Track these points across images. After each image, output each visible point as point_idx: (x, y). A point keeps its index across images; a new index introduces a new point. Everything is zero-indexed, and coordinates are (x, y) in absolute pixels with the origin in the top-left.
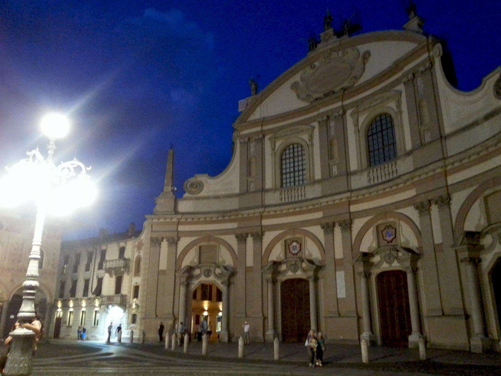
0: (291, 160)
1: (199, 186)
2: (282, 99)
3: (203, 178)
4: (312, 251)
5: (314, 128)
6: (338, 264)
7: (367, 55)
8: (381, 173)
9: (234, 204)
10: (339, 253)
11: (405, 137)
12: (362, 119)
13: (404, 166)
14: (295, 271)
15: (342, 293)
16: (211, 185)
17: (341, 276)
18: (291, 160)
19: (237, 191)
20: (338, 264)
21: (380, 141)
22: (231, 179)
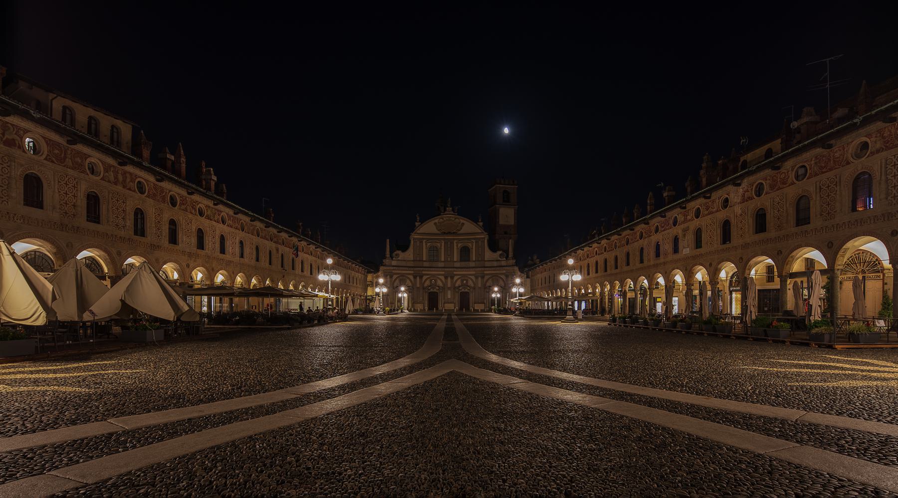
0: (434, 252)
1: (397, 255)
2: (430, 226)
3: (399, 252)
4: (440, 283)
6: (449, 288)
7: (463, 224)
8: (464, 264)
9: (411, 264)
10: (449, 286)
11: (473, 257)
13: (472, 264)
15: (449, 297)
16: (402, 255)
17: (449, 292)
18: (434, 252)
20: (449, 288)
21: (465, 253)
22: (409, 255)
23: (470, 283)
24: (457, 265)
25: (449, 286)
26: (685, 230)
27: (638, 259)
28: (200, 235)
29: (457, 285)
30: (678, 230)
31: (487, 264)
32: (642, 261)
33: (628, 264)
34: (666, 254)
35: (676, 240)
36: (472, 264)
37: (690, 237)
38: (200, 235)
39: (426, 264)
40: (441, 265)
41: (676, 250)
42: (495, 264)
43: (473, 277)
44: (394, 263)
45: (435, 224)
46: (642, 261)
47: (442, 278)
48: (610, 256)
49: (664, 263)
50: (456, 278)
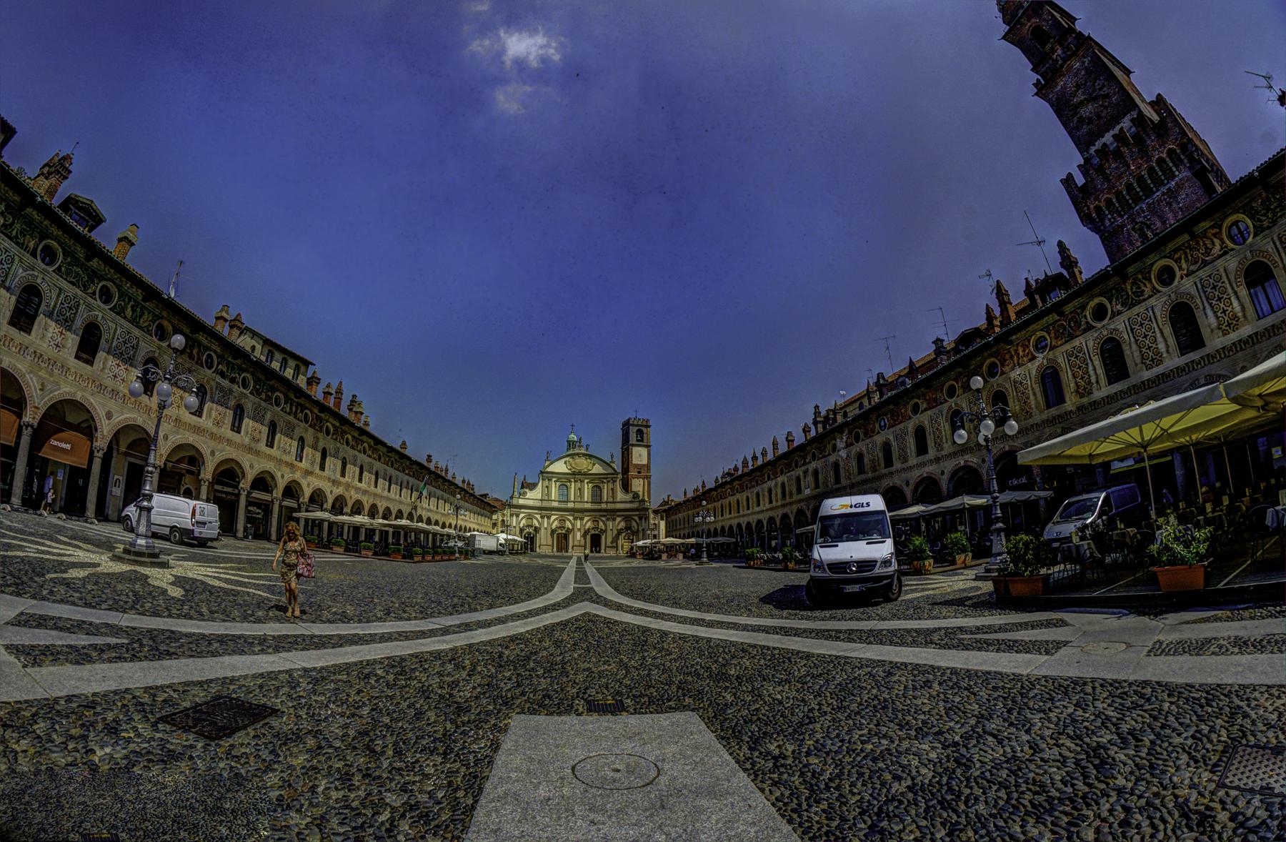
1: (525, 493)
4: (568, 525)
16: (530, 494)
26: (806, 472)
27: (767, 500)
30: (800, 471)
32: (771, 502)
33: (759, 505)
34: (791, 495)
35: (798, 479)
37: (810, 479)
39: (555, 504)
40: (570, 505)
41: (799, 491)
44: (521, 502)
46: (771, 502)
48: (741, 497)
49: (790, 504)
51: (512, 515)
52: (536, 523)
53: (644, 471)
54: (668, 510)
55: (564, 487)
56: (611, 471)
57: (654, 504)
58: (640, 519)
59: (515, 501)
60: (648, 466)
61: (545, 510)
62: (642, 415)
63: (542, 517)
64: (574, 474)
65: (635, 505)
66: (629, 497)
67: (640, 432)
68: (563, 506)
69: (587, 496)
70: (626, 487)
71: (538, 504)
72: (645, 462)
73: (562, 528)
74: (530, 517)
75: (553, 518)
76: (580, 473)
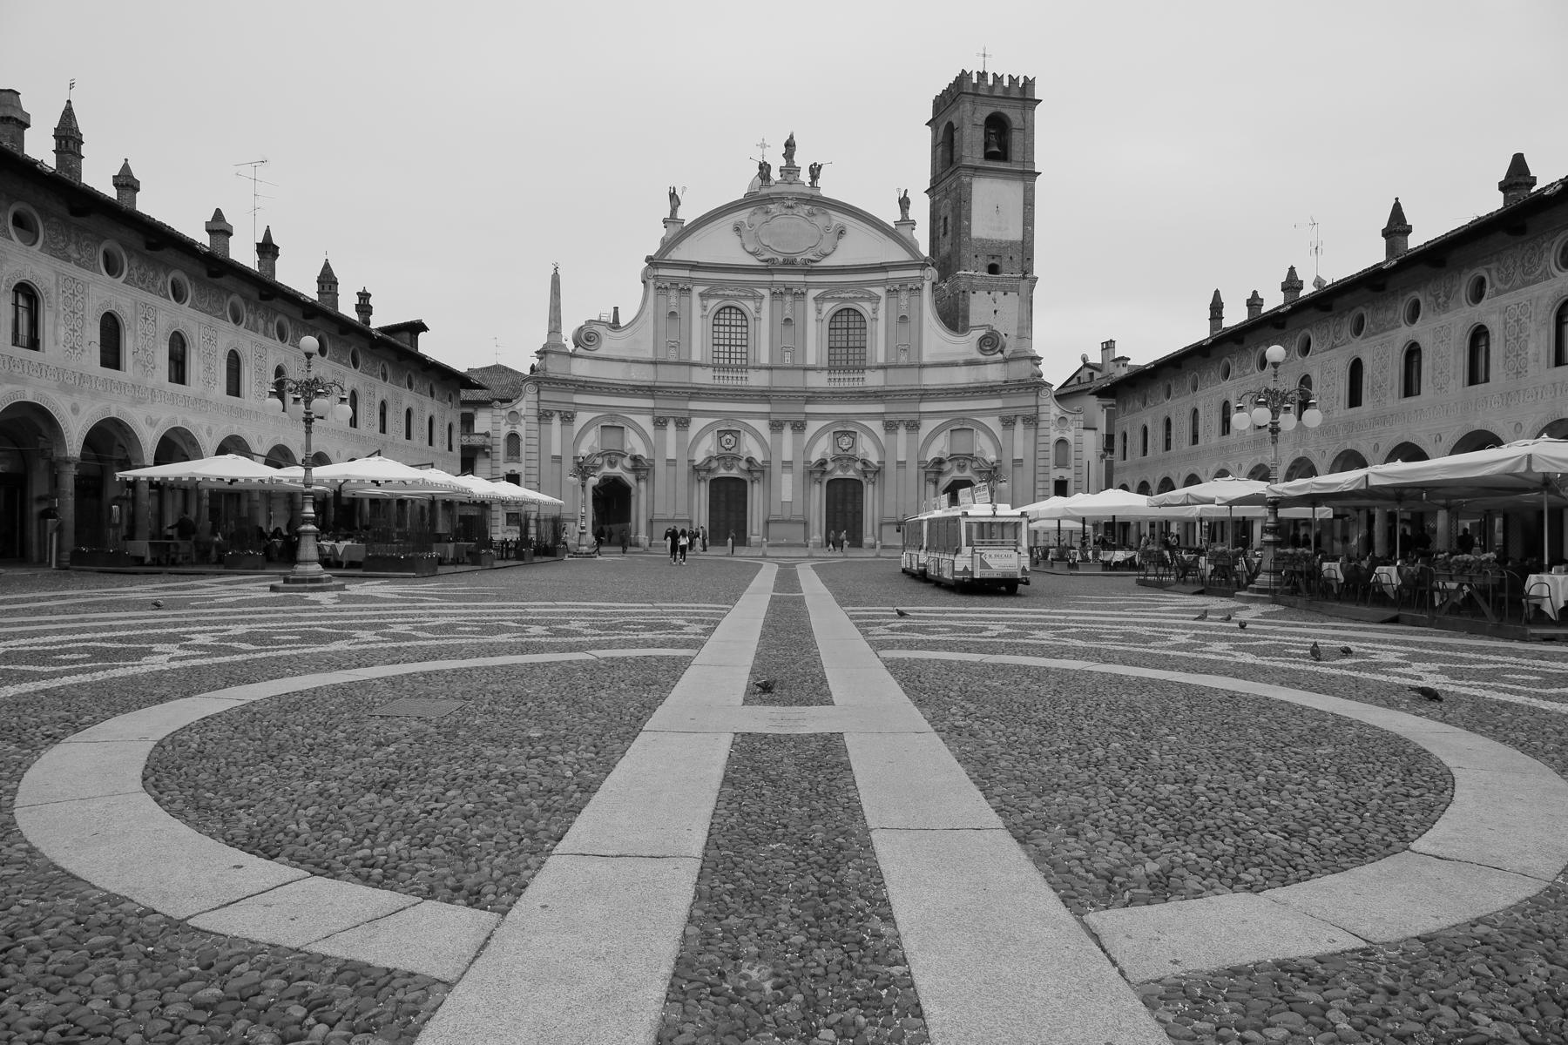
4: (750, 447)
5: (762, 297)
6: (787, 465)
12: (828, 308)
14: (730, 468)
19: (649, 355)
23: (867, 449)
24: (819, 381)
25: (787, 456)
28: (111, 328)
29: (815, 457)
31: (932, 379)
36: (874, 380)
38: (111, 328)
39: (703, 377)
40: (758, 380)
42: (962, 377)
43: (876, 426)
44: (581, 369)
45: (737, 229)
47: (762, 426)
50: (813, 426)
51: (544, 416)
52: (634, 444)
53: (1012, 265)
54: (1121, 386)
55: (729, 315)
56: (898, 255)
57: (1056, 373)
58: (1008, 423)
59: (555, 368)
60: (1025, 249)
61: (670, 400)
62: (1005, 65)
63: (660, 423)
64: (769, 268)
65: (993, 373)
66: (965, 345)
67: (998, 128)
68: (731, 381)
69: (815, 348)
70: (953, 318)
71: (643, 375)
72: (1015, 234)
73: (728, 459)
74: (613, 426)
75: (698, 424)
76: (789, 266)
